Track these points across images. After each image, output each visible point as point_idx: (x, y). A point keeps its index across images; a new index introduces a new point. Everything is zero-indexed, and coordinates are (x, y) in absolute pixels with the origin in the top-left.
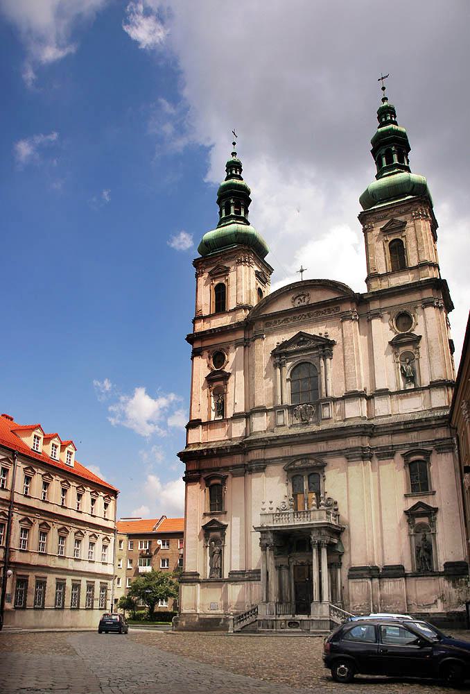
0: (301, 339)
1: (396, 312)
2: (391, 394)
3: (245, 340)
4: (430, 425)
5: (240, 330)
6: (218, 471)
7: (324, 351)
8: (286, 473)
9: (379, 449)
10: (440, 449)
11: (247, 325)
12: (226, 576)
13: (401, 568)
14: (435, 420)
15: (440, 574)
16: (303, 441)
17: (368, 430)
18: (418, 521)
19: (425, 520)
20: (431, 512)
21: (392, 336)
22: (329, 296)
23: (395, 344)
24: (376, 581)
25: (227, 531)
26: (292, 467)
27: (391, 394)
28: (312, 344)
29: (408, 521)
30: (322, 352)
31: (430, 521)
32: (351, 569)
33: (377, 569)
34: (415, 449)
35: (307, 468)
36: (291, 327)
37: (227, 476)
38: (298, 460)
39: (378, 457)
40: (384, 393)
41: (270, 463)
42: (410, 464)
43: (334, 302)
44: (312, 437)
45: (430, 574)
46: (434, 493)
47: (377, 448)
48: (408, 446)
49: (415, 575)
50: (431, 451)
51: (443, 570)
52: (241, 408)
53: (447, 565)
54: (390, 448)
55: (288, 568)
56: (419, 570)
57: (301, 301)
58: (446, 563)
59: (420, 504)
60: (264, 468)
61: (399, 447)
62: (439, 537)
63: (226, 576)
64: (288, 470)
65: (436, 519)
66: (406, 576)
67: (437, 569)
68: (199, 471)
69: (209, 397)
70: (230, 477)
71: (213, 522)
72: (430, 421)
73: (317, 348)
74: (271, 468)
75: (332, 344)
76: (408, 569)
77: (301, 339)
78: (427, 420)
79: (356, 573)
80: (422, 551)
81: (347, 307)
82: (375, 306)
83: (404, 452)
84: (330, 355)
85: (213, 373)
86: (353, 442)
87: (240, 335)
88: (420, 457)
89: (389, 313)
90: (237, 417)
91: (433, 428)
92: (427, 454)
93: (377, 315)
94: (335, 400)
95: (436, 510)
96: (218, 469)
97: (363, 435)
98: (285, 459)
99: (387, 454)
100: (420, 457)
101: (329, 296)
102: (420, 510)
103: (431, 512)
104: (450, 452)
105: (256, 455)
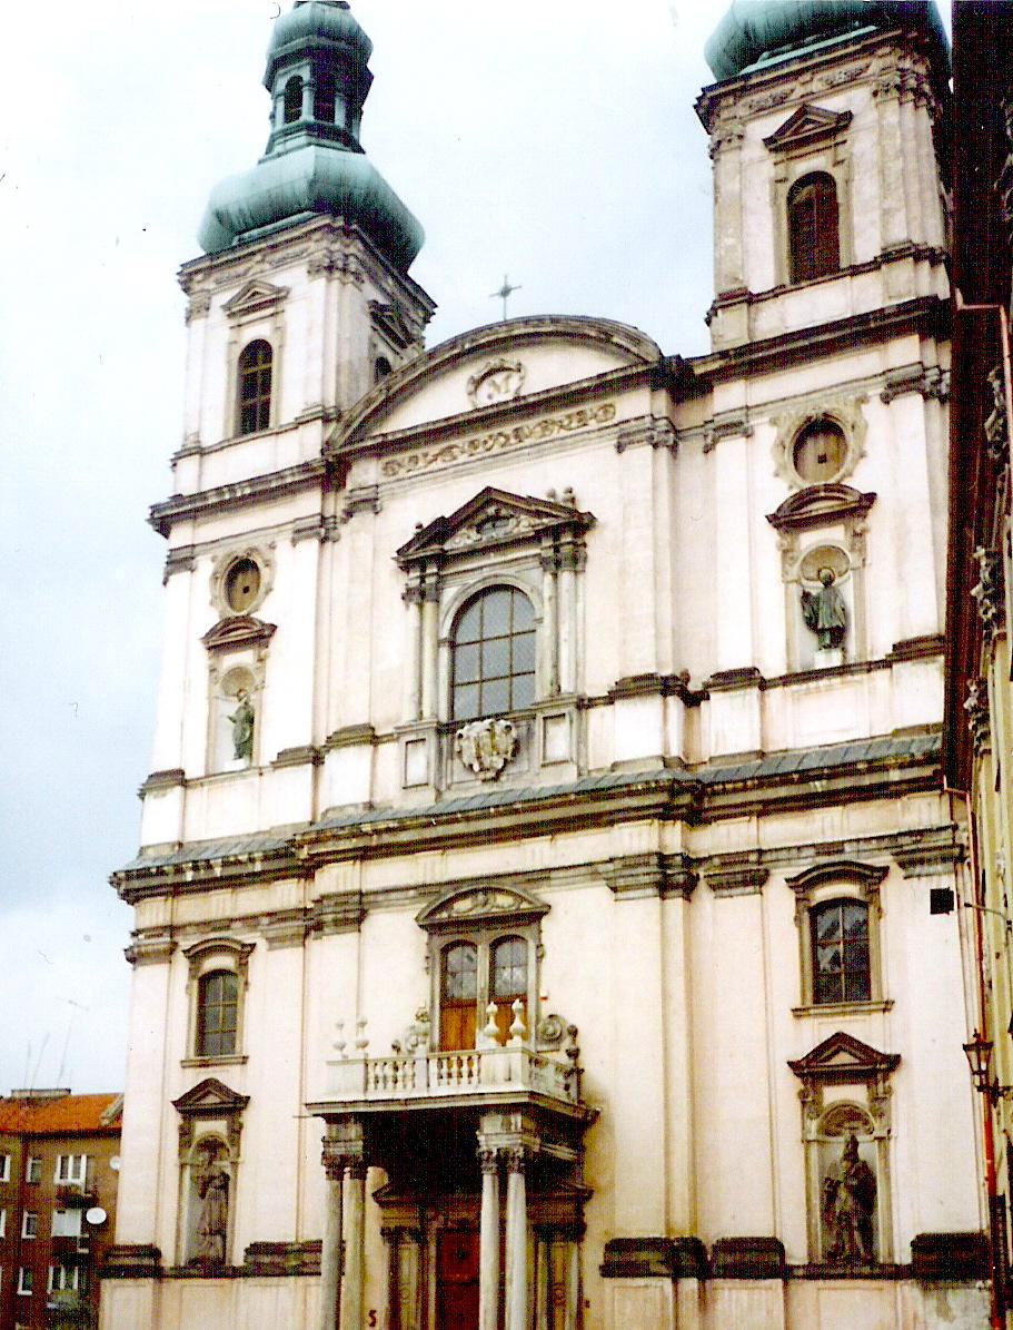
0: (491, 510)
1: (793, 418)
2: (764, 685)
3: (323, 519)
4: (886, 785)
5: (308, 488)
6: (228, 928)
7: (556, 549)
8: (424, 936)
9: (716, 861)
10: (913, 863)
11: (330, 473)
12: (238, 1258)
13: (774, 1246)
14: (902, 767)
15: (896, 1273)
16: (478, 834)
17: (685, 799)
18: (833, 1095)
19: (856, 1094)
20: (877, 1067)
21: (779, 493)
22: (582, 365)
23: (790, 520)
24: (690, 1285)
25: (249, 1117)
26: (445, 915)
27: (764, 685)
28: (524, 525)
29: (803, 1095)
30: (551, 553)
31: (875, 1099)
32: (615, 1246)
33: (694, 1246)
34: (833, 865)
35: (489, 921)
36: (462, 471)
37: (253, 946)
38: (465, 895)
39: (713, 888)
40: (746, 678)
41: (376, 905)
42: (817, 911)
43: (603, 387)
44: (505, 822)
45: (866, 1270)
46: (887, 1006)
47: (710, 858)
48: (812, 851)
49: (819, 1271)
50: (885, 870)
51: (904, 1256)
52: (303, 739)
53: (923, 1244)
54: (753, 857)
55: (420, 1237)
56: (832, 1256)
57: (498, 388)
58: (921, 1238)
59: (840, 1041)
60: (360, 921)
61: (783, 855)
62: (899, 1150)
63: (238, 1258)
64: (431, 926)
65: (888, 1091)
66: (785, 1273)
67: (891, 1255)
68: (173, 929)
69: (211, 699)
70: (262, 945)
71: (205, 1087)
72: (885, 769)
73: (536, 537)
74: (378, 921)
75: (580, 525)
76: (797, 1254)
77: (491, 510)
78: (874, 766)
79: (624, 1259)
80: (843, 1193)
81: (639, 404)
82: (729, 397)
83: (793, 872)
84: (577, 560)
85: (227, 626)
86: (637, 838)
87: (309, 504)
88: (850, 889)
89: (774, 422)
90: (287, 758)
91: (898, 795)
92: (872, 878)
93: (735, 427)
94: (584, 704)
95: (894, 1062)
96: (227, 923)
97: (666, 814)
98: (423, 889)
99: (747, 873)
100: (850, 889)
101: (582, 365)
102: (843, 1058)
103: (877, 1067)
104: (949, 873)
105: (335, 879)
